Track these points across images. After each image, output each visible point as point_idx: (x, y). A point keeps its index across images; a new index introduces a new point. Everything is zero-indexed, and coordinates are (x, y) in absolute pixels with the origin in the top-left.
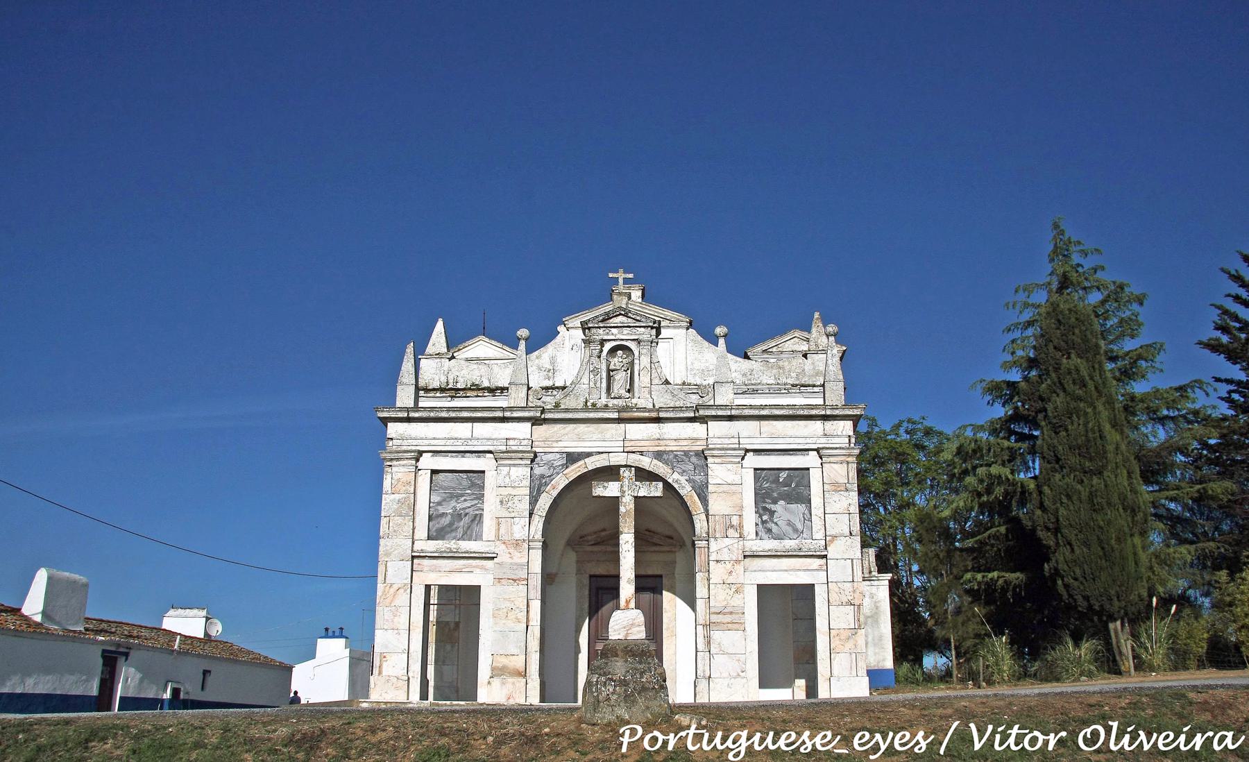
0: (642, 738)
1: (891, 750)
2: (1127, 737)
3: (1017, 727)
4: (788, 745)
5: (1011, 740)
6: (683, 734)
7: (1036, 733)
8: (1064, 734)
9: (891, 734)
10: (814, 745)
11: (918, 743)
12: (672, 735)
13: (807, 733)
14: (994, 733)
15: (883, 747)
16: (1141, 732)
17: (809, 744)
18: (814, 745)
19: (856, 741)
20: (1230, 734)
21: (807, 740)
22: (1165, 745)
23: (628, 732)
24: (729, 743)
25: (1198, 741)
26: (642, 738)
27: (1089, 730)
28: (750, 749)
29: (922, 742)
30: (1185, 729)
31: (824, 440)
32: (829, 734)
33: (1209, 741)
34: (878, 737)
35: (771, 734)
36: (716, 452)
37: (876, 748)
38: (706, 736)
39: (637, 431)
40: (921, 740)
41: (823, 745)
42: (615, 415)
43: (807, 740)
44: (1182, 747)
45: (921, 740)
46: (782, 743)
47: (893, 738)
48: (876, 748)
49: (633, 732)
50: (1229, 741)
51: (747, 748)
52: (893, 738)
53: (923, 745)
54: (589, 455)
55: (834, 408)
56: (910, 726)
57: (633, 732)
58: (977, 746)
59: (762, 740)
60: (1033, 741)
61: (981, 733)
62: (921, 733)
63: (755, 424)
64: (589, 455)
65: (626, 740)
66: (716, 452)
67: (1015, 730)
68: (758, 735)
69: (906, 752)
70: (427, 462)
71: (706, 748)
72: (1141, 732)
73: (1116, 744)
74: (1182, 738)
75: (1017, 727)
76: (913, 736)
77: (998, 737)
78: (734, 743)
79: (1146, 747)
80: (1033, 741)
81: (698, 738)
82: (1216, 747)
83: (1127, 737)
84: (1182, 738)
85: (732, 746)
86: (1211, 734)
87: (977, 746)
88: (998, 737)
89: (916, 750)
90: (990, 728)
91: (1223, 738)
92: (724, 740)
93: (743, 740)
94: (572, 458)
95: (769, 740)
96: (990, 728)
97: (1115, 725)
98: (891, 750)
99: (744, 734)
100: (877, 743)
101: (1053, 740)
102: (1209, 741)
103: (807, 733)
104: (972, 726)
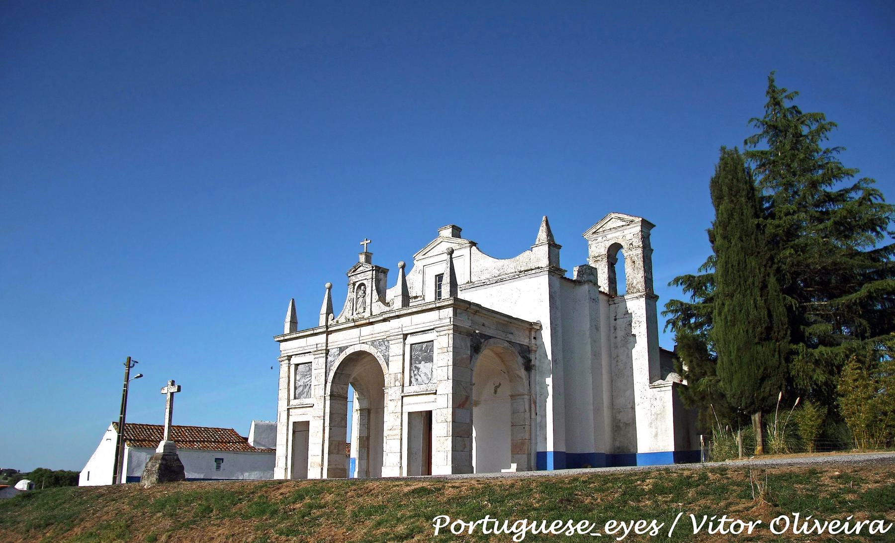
0: (450, 523)
1: (632, 534)
2: (806, 524)
3: (488, 516)
4: (556, 530)
5: (721, 527)
6: (480, 522)
7: (739, 521)
8: (759, 522)
9: (632, 522)
10: (576, 530)
11: (568, 528)
12: (472, 523)
13: (571, 521)
14: (708, 520)
15: (627, 532)
16: (816, 521)
17: (572, 529)
18: (576, 530)
19: (607, 528)
20: (881, 522)
21: (571, 527)
22: (556, 530)
23: (439, 521)
24: (513, 529)
25: (858, 527)
26: (450, 523)
27: (778, 519)
28: (528, 533)
29: (655, 528)
30: (807, 519)
31: (438, 322)
32: (587, 523)
33: (866, 527)
34: (623, 524)
35: (544, 522)
36: (392, 338)
37: (622, 532)
38: (497, 523)
39: (366, 330)
40: (655, 527)
41: (582, 530)
42: (353, 324)
43: (571, 527)
44: (846, 532)
45: (655, 527)
46: (552, 528)
47: (633, 527)
48: (622, 532)
49: (443, 521)
50: (881, 527)
51: (527, 533)
52: (633, 527)
53: (656, 530)
54: (347, 347)
55: (430, 303)
56: (648, 517)
57: (443, 521)
58: (696, 531)
59: (538, 527)
60: (737, 527)
61: (699, 518)
62: (655, 521)
63: (409, 318)
64: (347, 347)
65: (438, 527)
66: (392, 338)
67: (724, 519)
68: (535, 523)
69: (610, 535)
70: (294, 360)
71: (496, 532)
72: (816, 521)
73: (798, 530)
74: (847, 525)
75: (725, 517)
76: (648, 524)
77: (711, 524)
78: (517, 529)
79: (820, 532)
80: (737, 527)
81: (490, 526)
82: (871, 532)
83: (806, 524)
84: (847, 525)
85: (515, 531)
86: (867, 522)
87: (696, 531)
88: (711, 524)
89: (567, 534)
90: (705, 517)
91: (876, 525)
92: (509, 527)
93: (523, 527)
94: (342, 350)
95: (543, 526)
96: (705, 517)
97: (797, 515)
98: (632, 534)
99: (525, 522)
100: (622, 528)
101: (751, 527)
102: (866, 527)
103: (571, 521)
104: (692, 516)
